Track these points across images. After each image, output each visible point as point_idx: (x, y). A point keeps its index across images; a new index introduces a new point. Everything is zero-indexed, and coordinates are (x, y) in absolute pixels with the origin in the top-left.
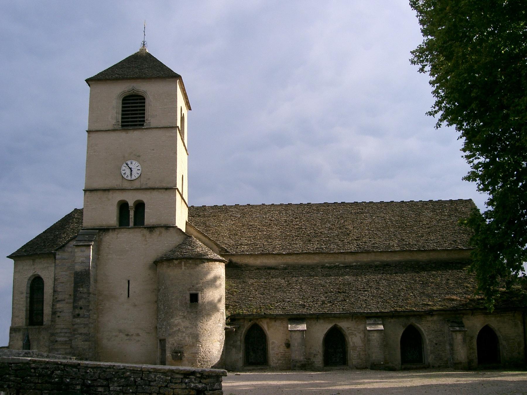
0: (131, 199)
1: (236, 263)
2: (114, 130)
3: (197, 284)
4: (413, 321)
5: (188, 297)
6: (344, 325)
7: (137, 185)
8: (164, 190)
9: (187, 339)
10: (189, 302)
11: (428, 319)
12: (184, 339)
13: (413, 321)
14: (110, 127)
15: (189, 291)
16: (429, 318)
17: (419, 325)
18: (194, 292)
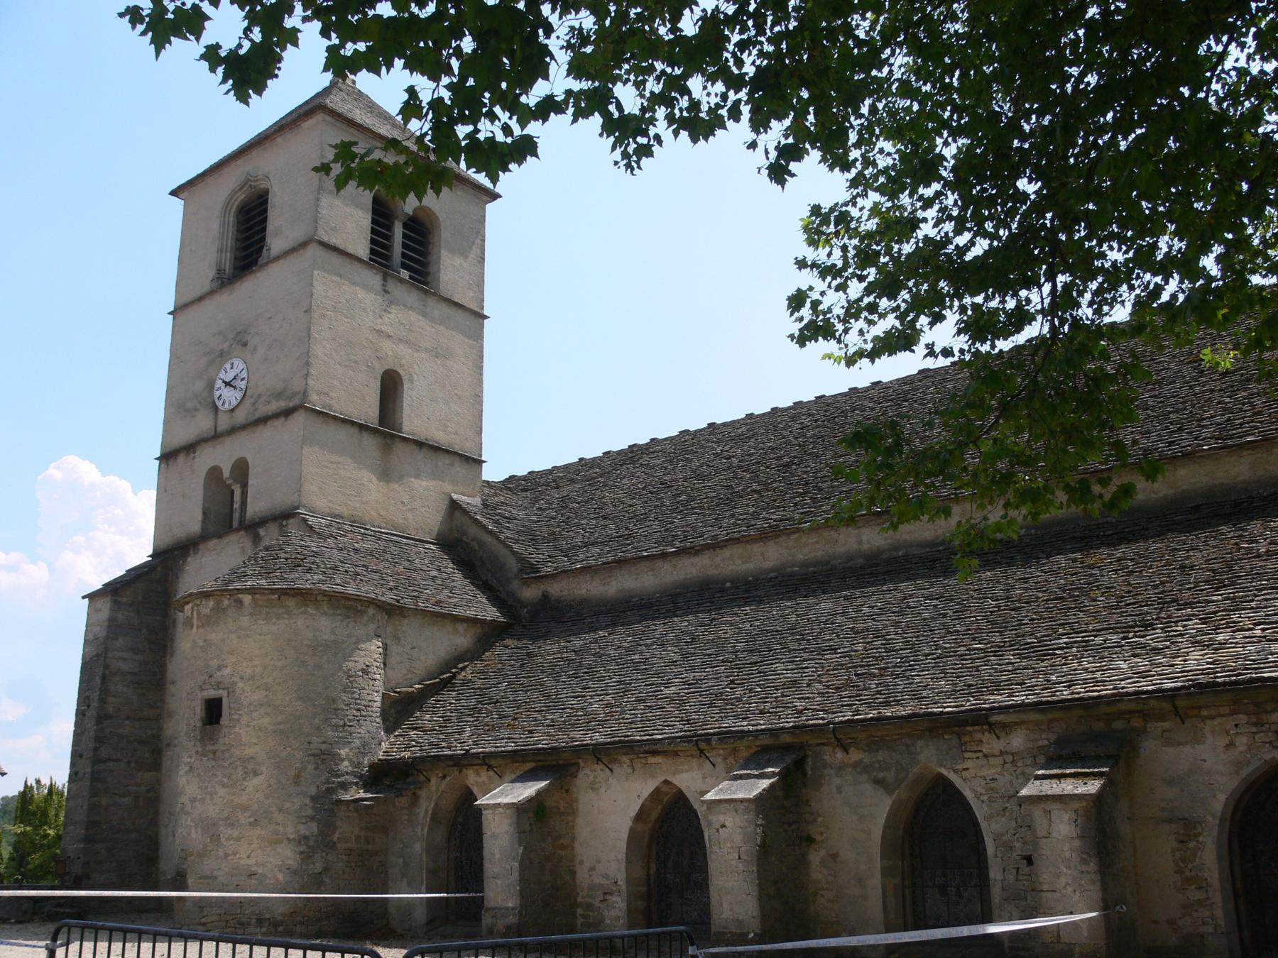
0: (221, 456)
1: (558, 601)
2: (211, 293)
3: (220, 668)
4: (929, 757)
5: (199, 710)
6: (688, 779)
7: (241, 417)
8: (282, 419)
9: (194, 835)
10: (199, 724)
11: (985, 749)
12: (189, 834)
13: (929, 757)
14: (207, 287)
15: (202, 690)
16: (992, 744)
17: (952, 777)
18: (211, 693)
